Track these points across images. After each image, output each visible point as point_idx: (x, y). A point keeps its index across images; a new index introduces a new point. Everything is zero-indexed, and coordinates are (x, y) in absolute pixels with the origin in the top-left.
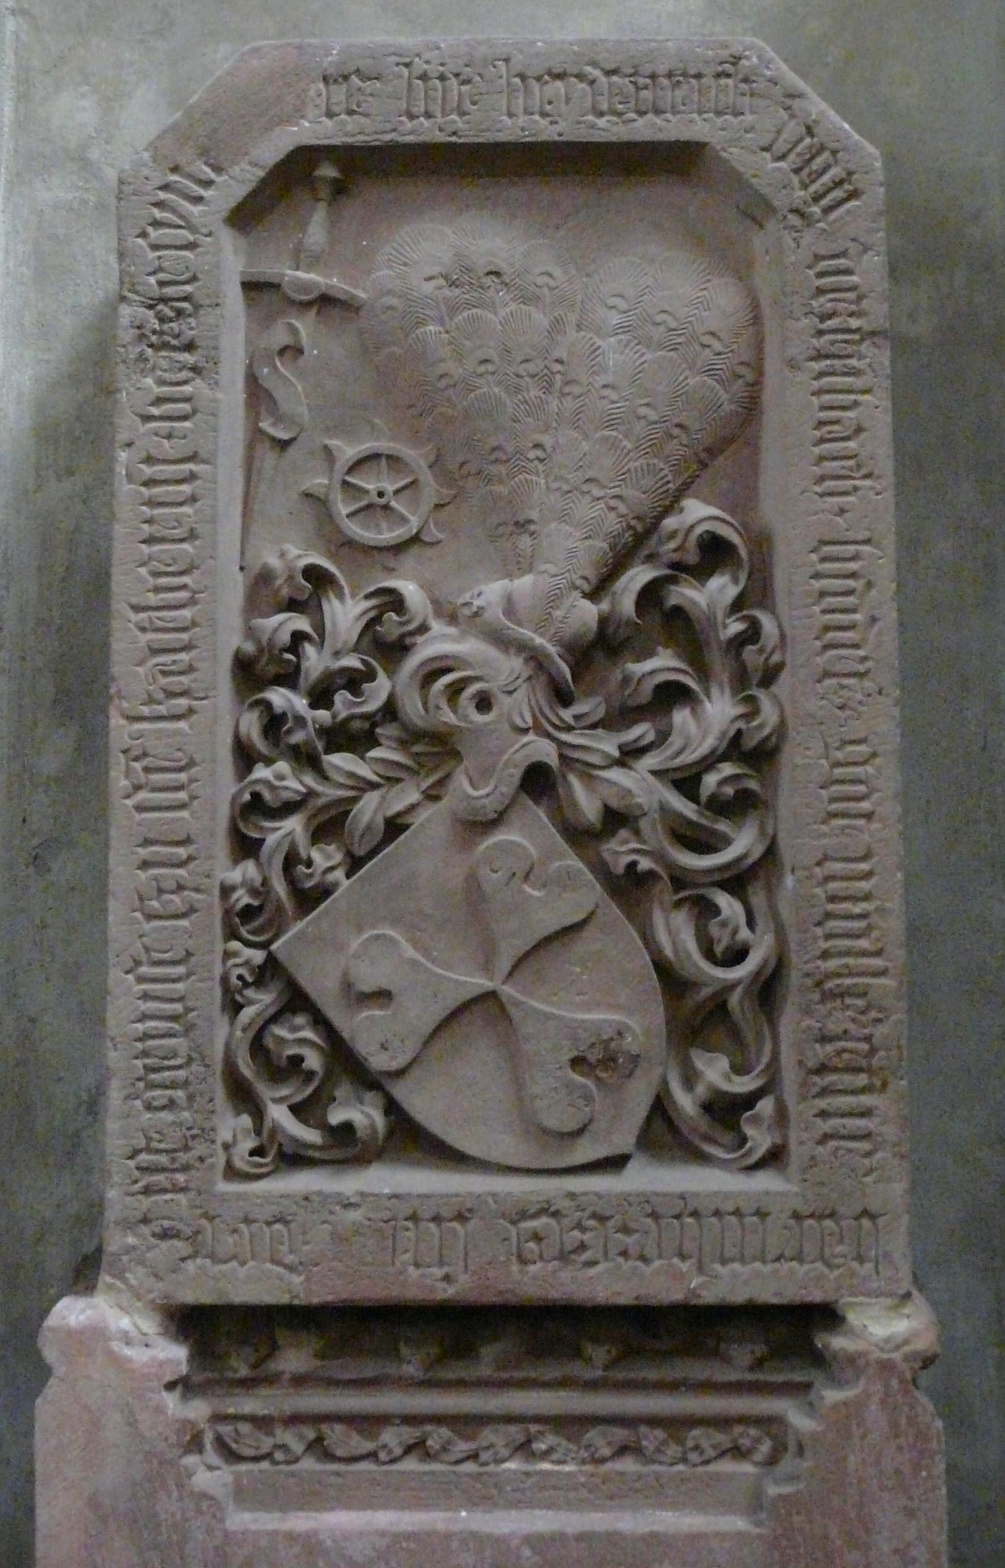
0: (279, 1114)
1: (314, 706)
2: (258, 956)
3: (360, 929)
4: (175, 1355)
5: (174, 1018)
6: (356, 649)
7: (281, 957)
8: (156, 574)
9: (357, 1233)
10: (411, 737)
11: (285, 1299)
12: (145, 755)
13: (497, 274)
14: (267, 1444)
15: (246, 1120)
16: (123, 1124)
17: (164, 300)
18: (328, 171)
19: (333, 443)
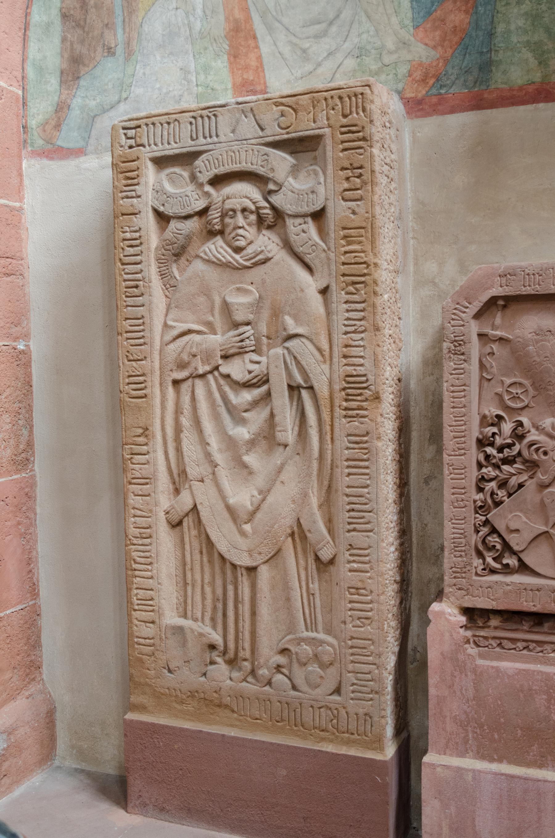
0: (489, 560)
1: (498, 452)
2: (484, 518)
3: (511, 512)
4: (463, 619)
5: (461, 534)
6: (510, 437)
7: (490, 519)
10: (525, 461)
11: (491, 608)
12: (453, 465)
13: (550, 331)
14: (487, 643)
16: (449, 560)
17: (456, 341)
18: (501, 302)
19: (503, 379)
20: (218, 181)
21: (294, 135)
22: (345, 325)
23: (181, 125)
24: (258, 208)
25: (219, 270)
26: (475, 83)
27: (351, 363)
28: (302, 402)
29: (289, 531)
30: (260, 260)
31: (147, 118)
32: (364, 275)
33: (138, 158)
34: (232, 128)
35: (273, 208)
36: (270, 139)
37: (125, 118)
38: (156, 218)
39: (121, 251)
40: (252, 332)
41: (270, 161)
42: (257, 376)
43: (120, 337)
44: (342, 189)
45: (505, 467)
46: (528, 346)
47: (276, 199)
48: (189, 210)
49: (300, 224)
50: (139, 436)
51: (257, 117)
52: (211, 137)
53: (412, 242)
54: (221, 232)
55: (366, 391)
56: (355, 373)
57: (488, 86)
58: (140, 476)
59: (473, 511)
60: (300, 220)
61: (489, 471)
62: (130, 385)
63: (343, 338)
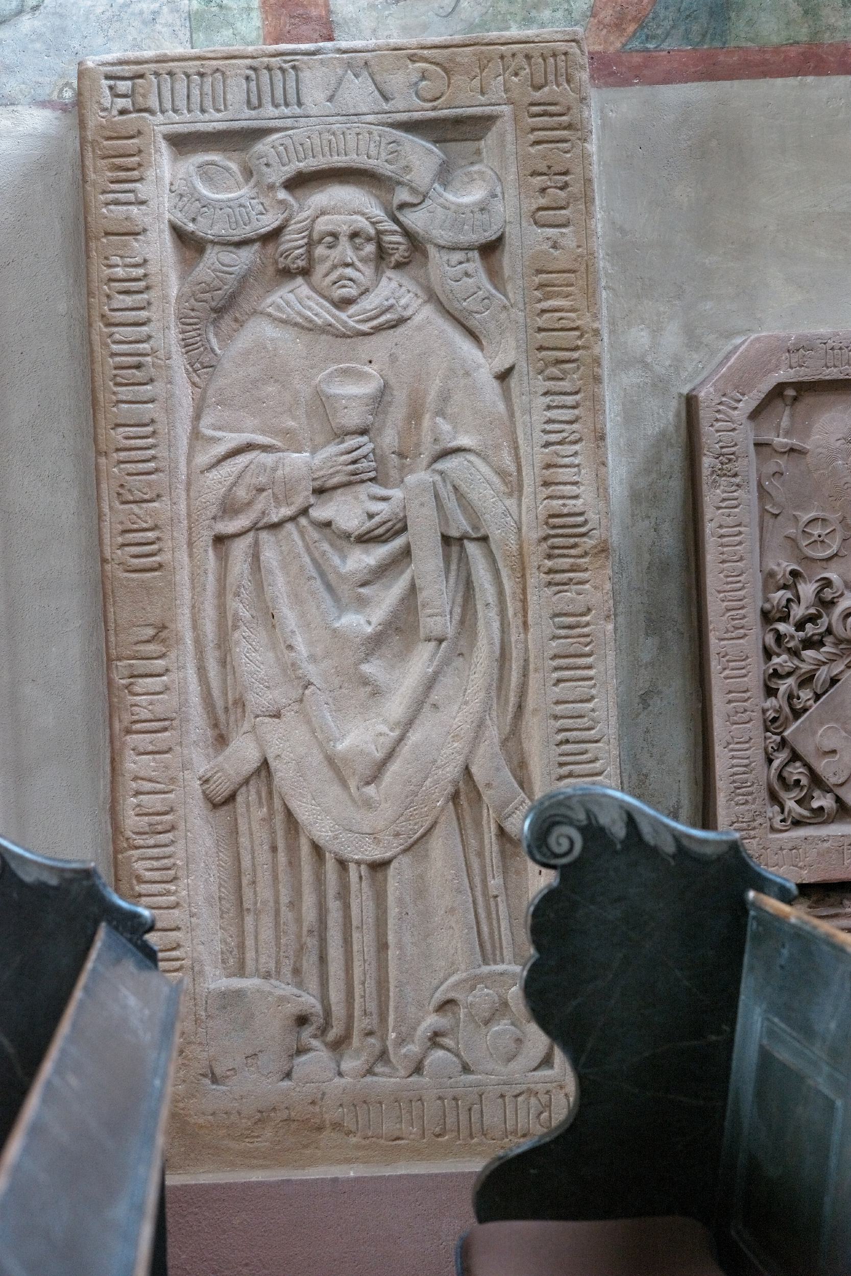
0: (790, 804)
1: (797, 630)
3: (822, 724)
5: (745, 766)
8: (728, 576)
9: (828, 852)
12: (726, 655)
15: (777, 808)
17: (723, 455)
18: (790, 392)
20: (300, 182)
21: (446, 112)
22: (544, 431)
23: (228, 81)
24: (379, 233)
25: (310, 336)
26: (704, 36)
27: (558, 494)
28: (467, 563)
29: (450, 789)
30: (387, 322)
31: (157, 62)
32: (576, 348)
33: (140, 132)
34: (329, 93)
35: (407, 233)
36: (404, 117)
37: (110, 57)
38: (174, 242)
39: (105, 300)
40: (371, 446)
41: (403, 153)
42: (385, 523)
43: (103, 460)
44: (535, 206)
45: (809, 654)
46: (835, 459)
47: (412, 219)
48: (246, 232)
49: (461, 263)
50: (148, 641)
51: (378, 78)
52: (287, 105)
53: (604, 294)
54: (305, 272)
55: (585, 539)
56: (565, 511)
57: (725, 43)
58: (149, 716)
59: (762, 728)
60: (458, 256)
61: (781, 660)
62: (127, 549)
63: (542, 453)
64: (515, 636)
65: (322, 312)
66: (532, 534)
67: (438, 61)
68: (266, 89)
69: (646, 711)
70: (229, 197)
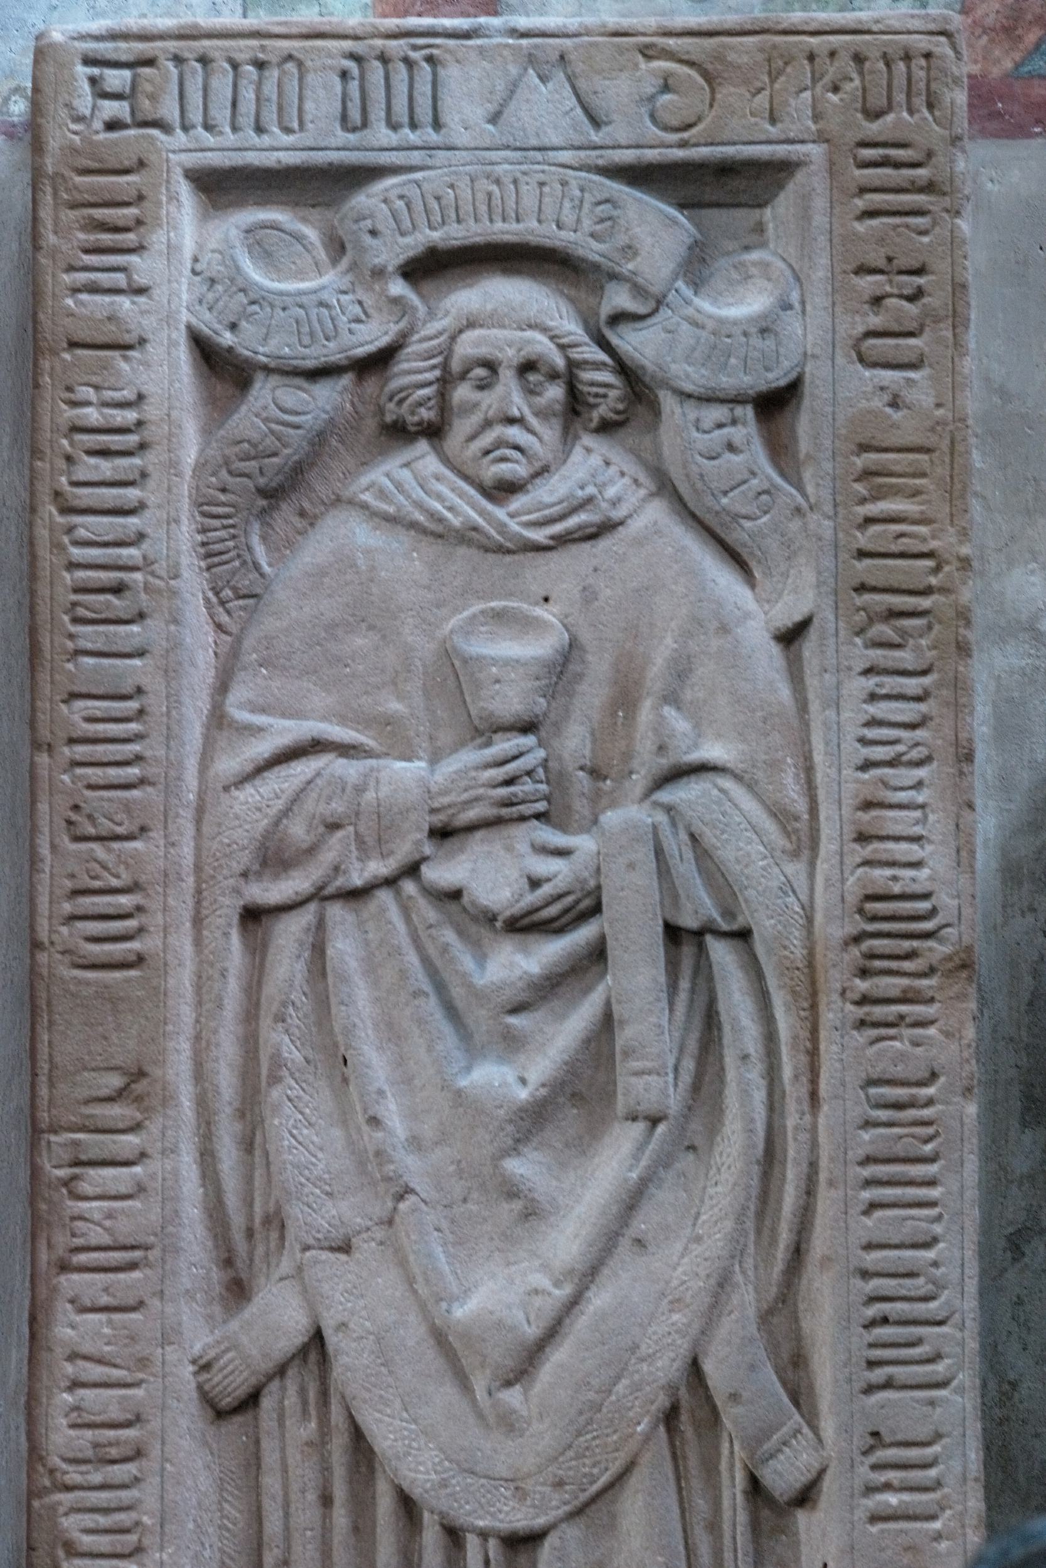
20: (432, 267)
22: (864, 741)
23: (310, 78)
24: (572, 364)
25: (438, 547)
27: (884, 857)
28: (710, 979)
29: (662, 1401)
30: (580, 527)
32: (927, 591)
34: (492, 108)
35: (624, 369)
36: (627, 156)
38: (196, 367)
39: (62, 464)
40: (541, 753)
41: (622, 222)
42: (560, 897)
43: (43, 759)
44: (861, 329)
47: (634, 342)
48: (328, 352)
49: (720, 426)
50: (110, 1099)
51: (582, 84)
52: (414, 126)
54: (434, 432)
55: (931, 943)
56: (897, 889)
58: (106, 1240)
60: (718, 413)
62: (80, 925)
63: (857, 781)
64: (793, 1118)
65: (462, 506)
66: (833, 929)
67: (693, 58)
68: (378, 94)
69: (1018, 1266)
70: (301, 288)
